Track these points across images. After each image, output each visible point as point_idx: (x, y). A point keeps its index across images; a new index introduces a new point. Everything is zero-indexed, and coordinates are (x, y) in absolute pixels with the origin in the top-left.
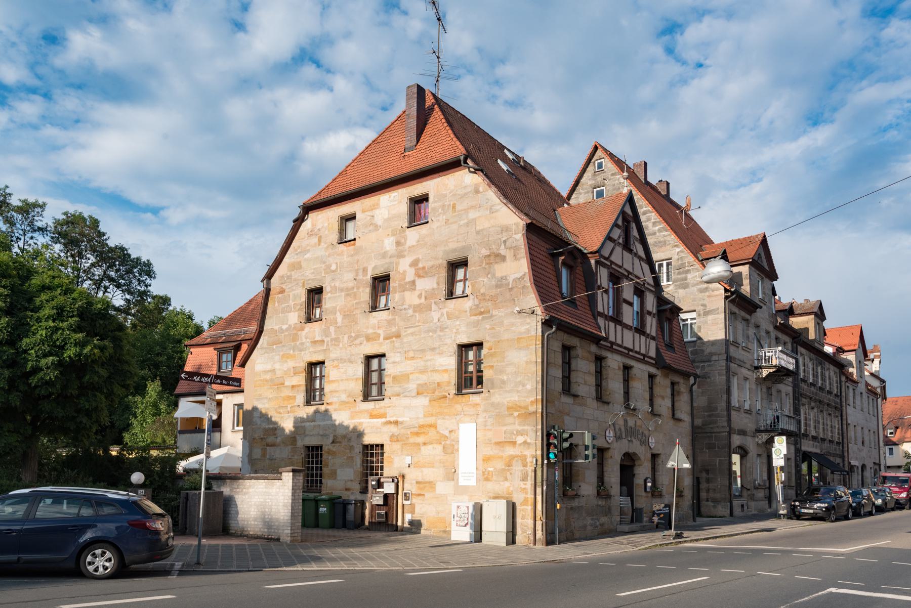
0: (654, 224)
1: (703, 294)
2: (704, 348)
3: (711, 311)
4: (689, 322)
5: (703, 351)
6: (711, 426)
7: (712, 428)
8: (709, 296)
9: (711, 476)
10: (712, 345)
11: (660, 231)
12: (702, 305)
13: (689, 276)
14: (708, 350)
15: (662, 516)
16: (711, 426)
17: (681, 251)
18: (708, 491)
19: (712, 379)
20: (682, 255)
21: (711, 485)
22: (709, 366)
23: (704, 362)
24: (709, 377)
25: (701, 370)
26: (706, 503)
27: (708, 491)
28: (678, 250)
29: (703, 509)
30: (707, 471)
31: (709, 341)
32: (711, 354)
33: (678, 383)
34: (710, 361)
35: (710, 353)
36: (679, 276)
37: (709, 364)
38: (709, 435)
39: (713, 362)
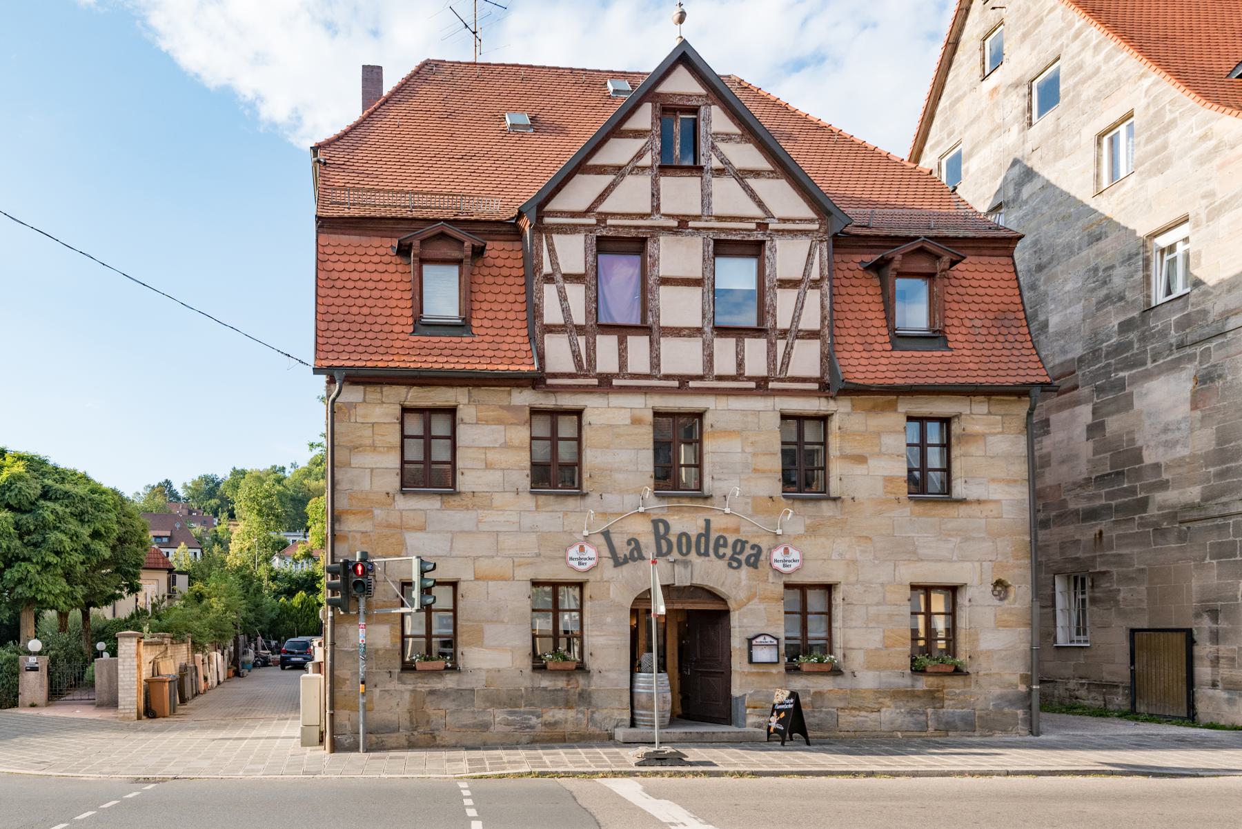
0: (1097, 48)
1: (1206, 167)
2: (1208, 305)
3: (1226, 202)
4: (1181, 248)
5: (1205, 312)
6: (1224, 499)
7: (1225, 504)
8: (1221, 167)
9: (1223, 625)
10: (1229, 291)
11: (1108, 58)
12: (1203, 197)
13: (1173, 136)
14: (1216, 307)
15: (783, 715)
16: (1224, 499)
17: (1156, 83)
18: (1215, 662)
19: (1229, 378)
20: (1156, 90)
21: (1222, 647)
22: (1222, 346)
23: (1210, 339)
24: (1220, 376)
25: (1201, 363)
26: (1211, 692)
27: (1215, 662)
28: (1146, 82)
29: (1201, 707)
30: (1214, 614)
31: (1221, 283)
32: (1226, 315)
33: (958, 416)
34: (1223, 334)
35: (1221, 315)
36: (1150, 147)
37: (1220, 340)
38: (1219, 522)
39: (1230, 335)
